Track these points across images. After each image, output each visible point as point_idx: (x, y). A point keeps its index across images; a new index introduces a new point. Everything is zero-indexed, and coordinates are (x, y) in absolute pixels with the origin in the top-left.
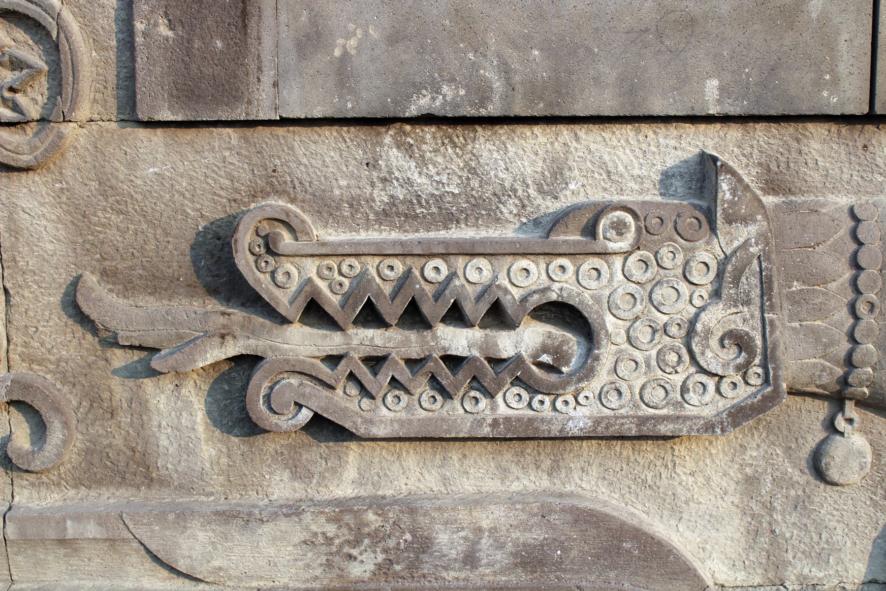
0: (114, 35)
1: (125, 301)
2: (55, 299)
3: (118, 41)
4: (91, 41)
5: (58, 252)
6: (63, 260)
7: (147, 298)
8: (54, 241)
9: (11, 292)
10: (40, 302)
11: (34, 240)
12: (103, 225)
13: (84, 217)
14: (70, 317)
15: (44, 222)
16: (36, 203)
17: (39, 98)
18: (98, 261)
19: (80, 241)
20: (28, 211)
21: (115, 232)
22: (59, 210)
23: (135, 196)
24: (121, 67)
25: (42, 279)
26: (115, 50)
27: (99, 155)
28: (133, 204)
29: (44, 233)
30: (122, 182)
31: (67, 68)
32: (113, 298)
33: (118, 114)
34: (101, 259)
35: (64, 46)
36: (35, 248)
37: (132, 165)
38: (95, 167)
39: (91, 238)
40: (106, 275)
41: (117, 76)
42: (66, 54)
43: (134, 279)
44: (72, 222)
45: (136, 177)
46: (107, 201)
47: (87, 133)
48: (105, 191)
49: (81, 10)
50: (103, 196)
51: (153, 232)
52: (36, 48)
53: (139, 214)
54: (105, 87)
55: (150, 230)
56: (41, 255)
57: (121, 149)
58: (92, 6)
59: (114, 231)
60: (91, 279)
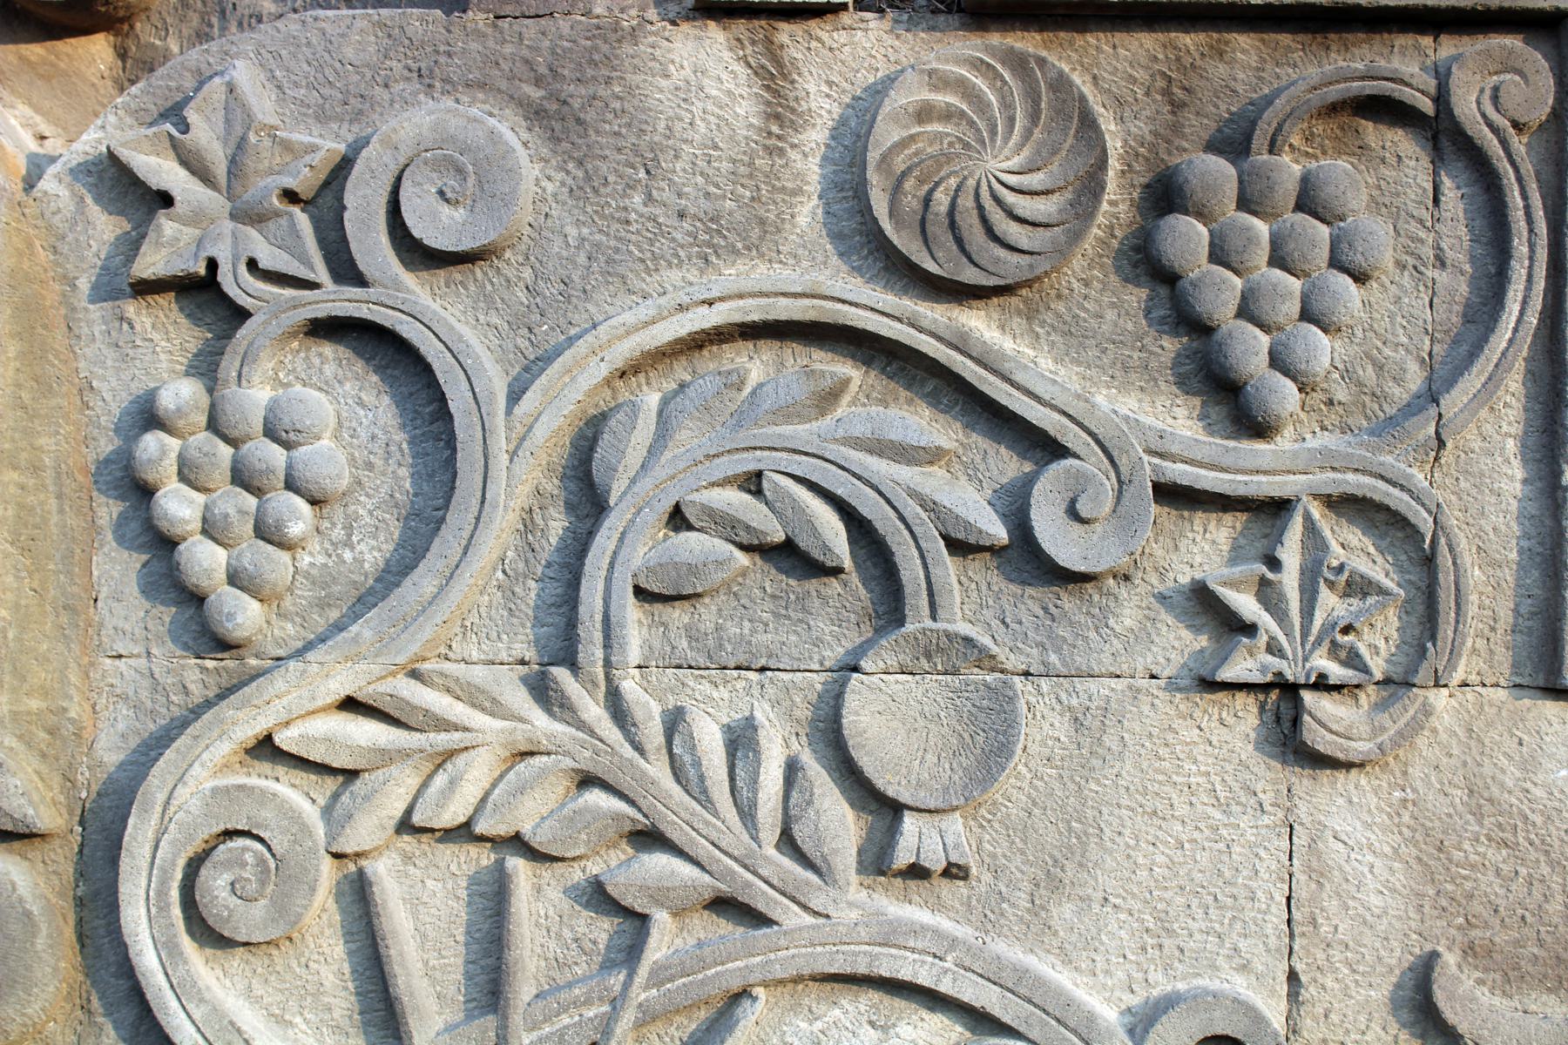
0: (1514, 542)
1: (1504, 1001)
2: (1380, 993)
3: (1520, 552)
4: (1474, 551)
5: (1390, 911)
6: (1398, 925)
7: (1544, 997)
8: (1385, 892)
9: (1303, 978)
10: (1351, 997)
11: (1353, 889)
12: (1473, 867)
13: (1440, 850)
14: (1404, 1025)
15: (1370, 858)
16: (1358, 825)
17: (1382, 644)
18: (1460, 928)
19: (1431, 892)
20: (1344, 837)
21: (1492, 879)
22: (1397, 838)
23: (1532, 816)
24: (1522, 596)
25: (1359, 957)
26: (1515, 567)
27: (1473, 743)
28: (1528, 831)
29: (1369, 876)
30: (1510, 792)
31: (1449, 596)
32: (1484, 996)
33: (1512, 674)
34: (1466, 925)
35: (1444, 559)
36: (1351, 903)
37: (1529, 765)
38: (1465, 764)
39: (1449, 887)
40: (1469, 950)
41: (1516, 611)
42: (1448, 573)
43: (1523, 963)
44: (1419, 860)
45: (1535, 784)
46: (1481, 825)
47: (1456, 705)
48: (1480, 807)
49: (1460, 499)
50: (1474, 814)
51: (1560, 881)
52: (1379, 559)
53: (1536, 850)
54: (1493, 629)
55: (1555, 878)
56: (1360, 916)
57: (1512, 735)
58: (1481, 492)
59: (1491, 876)
60: (1450, 959)
